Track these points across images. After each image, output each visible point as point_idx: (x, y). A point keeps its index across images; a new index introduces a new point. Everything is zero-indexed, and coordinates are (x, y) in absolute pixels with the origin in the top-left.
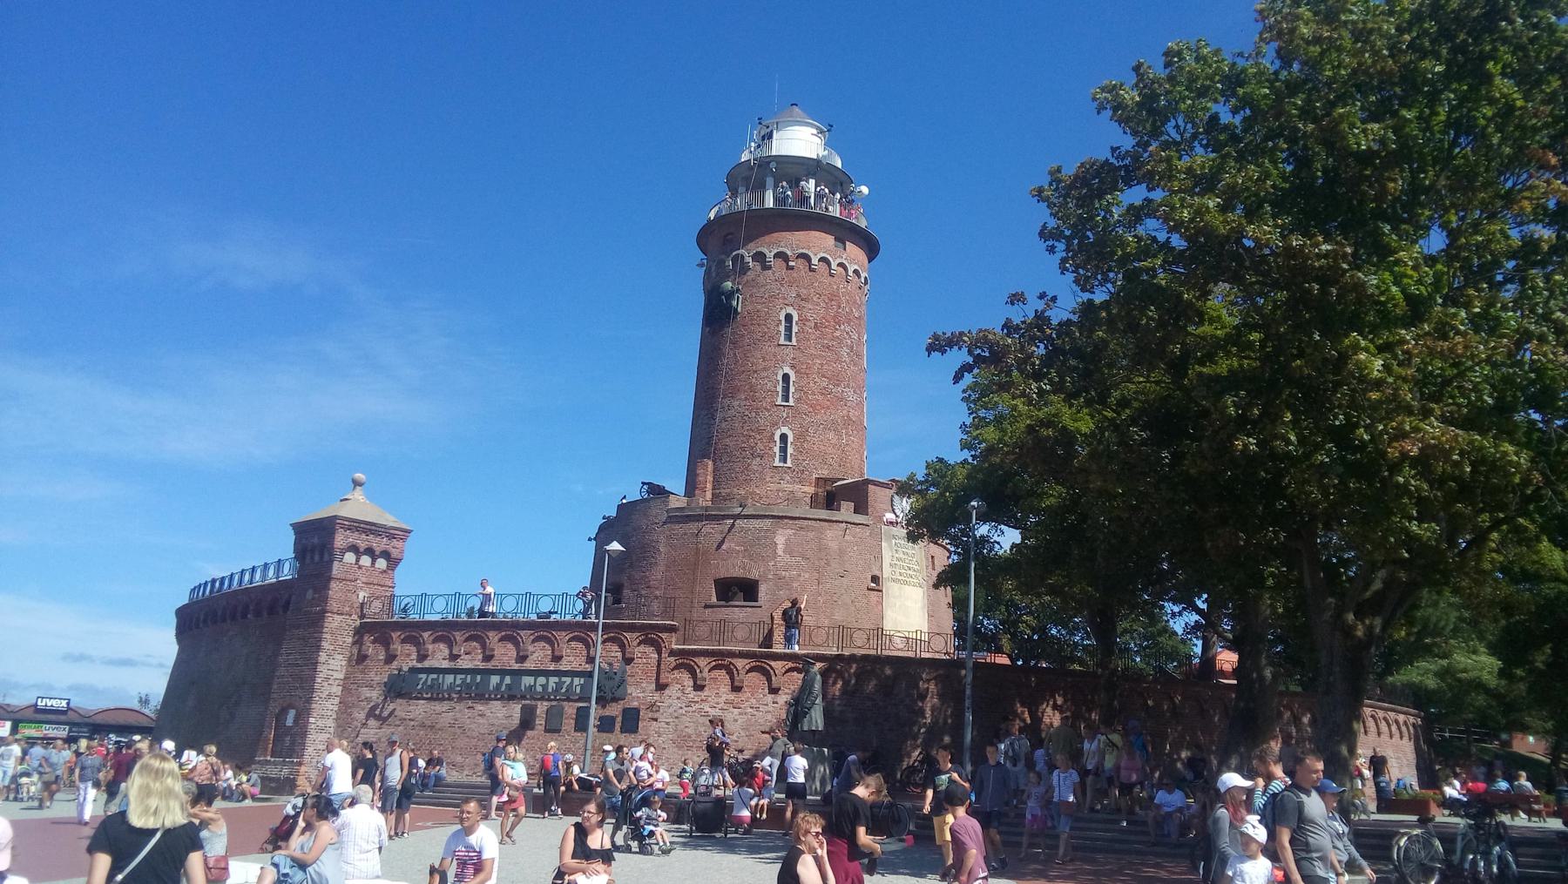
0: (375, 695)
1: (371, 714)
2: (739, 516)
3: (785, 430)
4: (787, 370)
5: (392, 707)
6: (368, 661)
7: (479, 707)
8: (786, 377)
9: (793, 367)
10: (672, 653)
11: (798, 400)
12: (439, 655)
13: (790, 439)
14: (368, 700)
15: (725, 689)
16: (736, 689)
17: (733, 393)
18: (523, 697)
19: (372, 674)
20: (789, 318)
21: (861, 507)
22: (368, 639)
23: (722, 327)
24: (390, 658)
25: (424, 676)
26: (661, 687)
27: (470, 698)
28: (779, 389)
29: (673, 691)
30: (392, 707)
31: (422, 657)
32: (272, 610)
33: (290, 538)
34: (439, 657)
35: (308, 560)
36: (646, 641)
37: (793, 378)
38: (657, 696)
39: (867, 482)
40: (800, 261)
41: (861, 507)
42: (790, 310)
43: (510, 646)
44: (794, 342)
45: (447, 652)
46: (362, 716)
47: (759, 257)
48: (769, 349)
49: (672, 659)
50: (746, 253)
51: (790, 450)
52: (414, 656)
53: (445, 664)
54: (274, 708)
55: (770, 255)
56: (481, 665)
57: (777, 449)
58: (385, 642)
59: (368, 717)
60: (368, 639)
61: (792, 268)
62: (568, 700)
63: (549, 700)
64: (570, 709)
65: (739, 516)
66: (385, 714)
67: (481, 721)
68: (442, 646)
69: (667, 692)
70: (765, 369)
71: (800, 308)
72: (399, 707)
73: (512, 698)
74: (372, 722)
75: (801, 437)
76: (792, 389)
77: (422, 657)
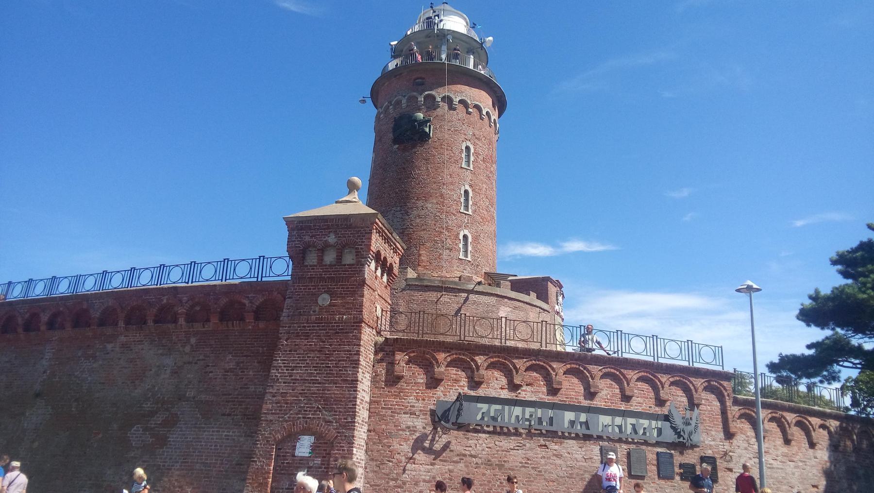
0: (421, 424)
1: (418, 445)
2: (472, 292)
3: (466, 232)
4: (467, 187)
5: (444, 439)
6: (402, 384)
7: (553, 446)
8: (466, 192)
9: (471, 186)
10: (736, 402)
11: (474, 211)
12: (496, 384)
13: (470, 240)
14: (412, 430)
15: (780, 441)
16: (787, 442)
17: (427, 197)
18: (600, 438)
19: (412, 400)
20: (468, 148)
21: (543, 296)
22: (401, 357)
23: (414, 146)
24: (434, 382)
25: (484, 407)
26: (729, 435)
27: (541, 435)
28: (462, 200)
29: (739, 440)
30: (444, 439)
31: (475, 384)
32: (224, 316)
33: (284, 233)
34: (495, 385)
35: (312, 259)
36: (709, 389)
37: (471, 194)
38: (727, 446)
39: (548, 279)
40: (475, 110)
41: (543, 296)
42: (469, 144)
43: (575, 380)
44: (471, 168)
45: (504, 381)
46: (406, 448)
47: (449, 100)
48: (454, 168)
49: (736, 408)
50: (439, 94)
51: (470, 248)
52: (464, 382)
53: (505, 394)
54: (271, 429)
55: (456, 100)
56: (548, 399)
57: (461, 246)
58: (428, 366)
59: (414, 449)
60: (401, 357)
61: (470, 113)
62: (646, 443)
63: (627, 442)
64: (651, 454)
65: (472, 292)
66: (438, 446)
67: (558, 462)
68: (497, 374)
69: (734, 441)
70: (452, 184)
71: (475, 144)
72: (456, 440)
73: (587, 438)
74: (420, 456)
75: (476, 239)
76: (470, 203)
77: (475, 384)
